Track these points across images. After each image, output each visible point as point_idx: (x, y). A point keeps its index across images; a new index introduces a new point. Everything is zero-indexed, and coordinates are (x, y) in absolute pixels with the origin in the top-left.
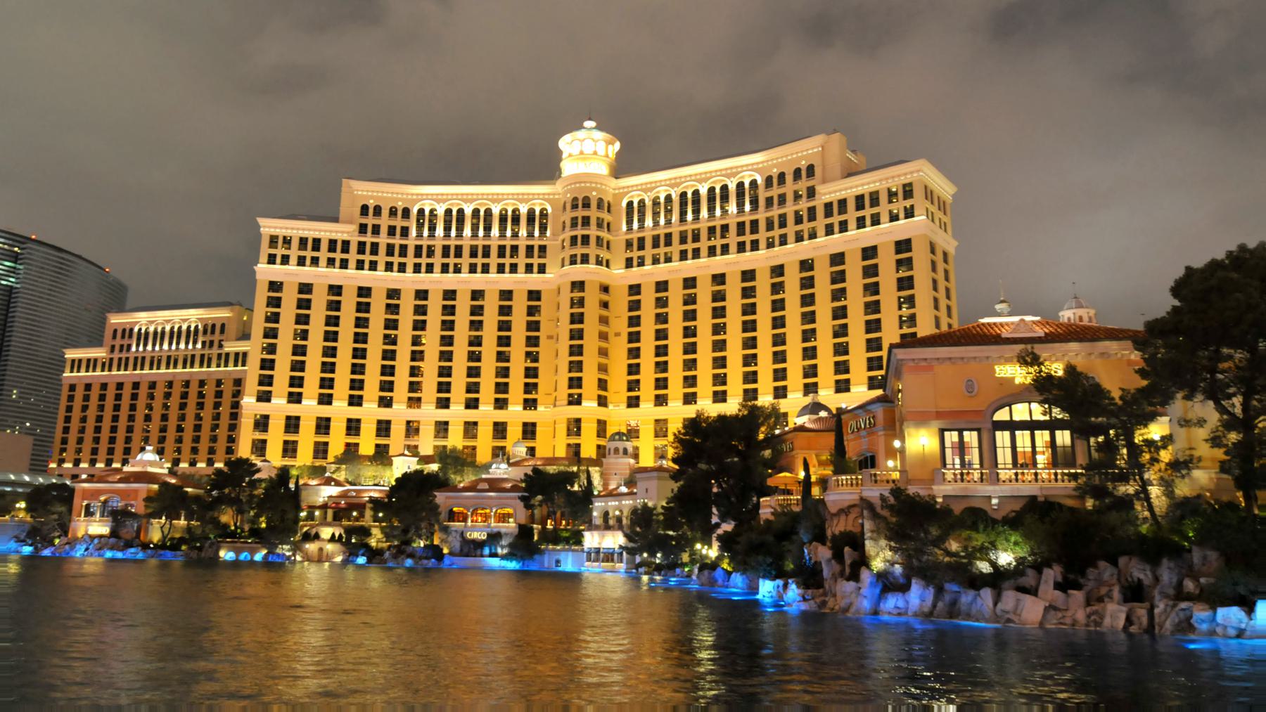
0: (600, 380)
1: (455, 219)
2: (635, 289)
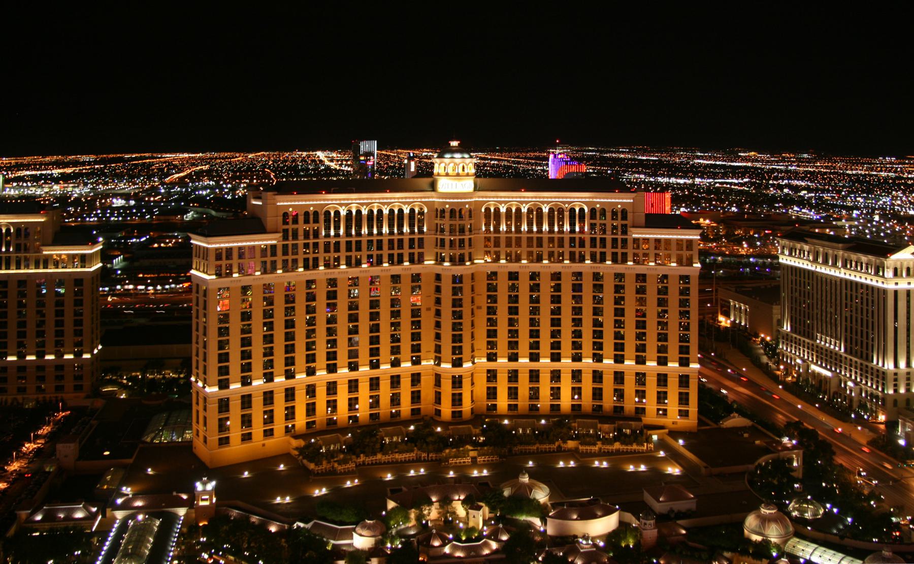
1: (355, 219)
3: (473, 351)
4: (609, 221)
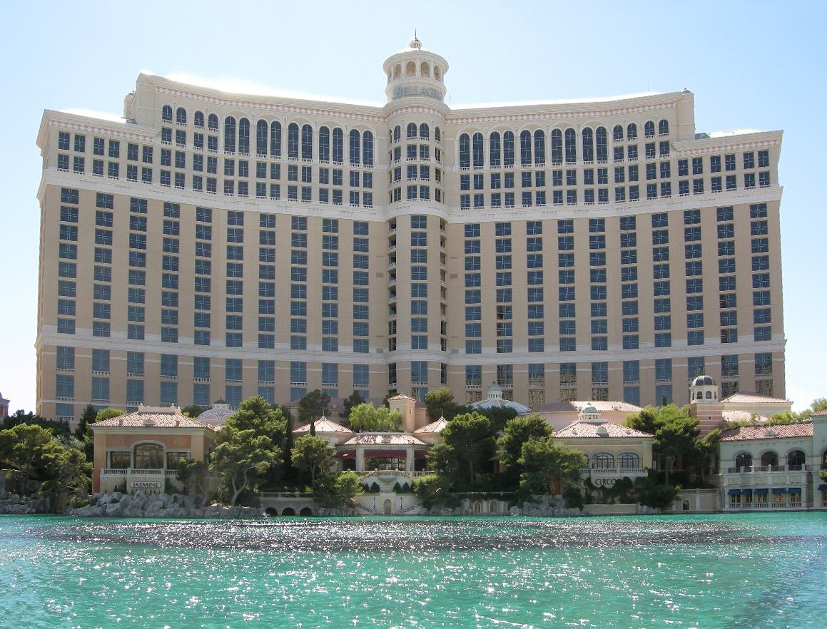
0: (443, 324)
2: (472, 229)
3: (443, 332)
4: (641, 140)
